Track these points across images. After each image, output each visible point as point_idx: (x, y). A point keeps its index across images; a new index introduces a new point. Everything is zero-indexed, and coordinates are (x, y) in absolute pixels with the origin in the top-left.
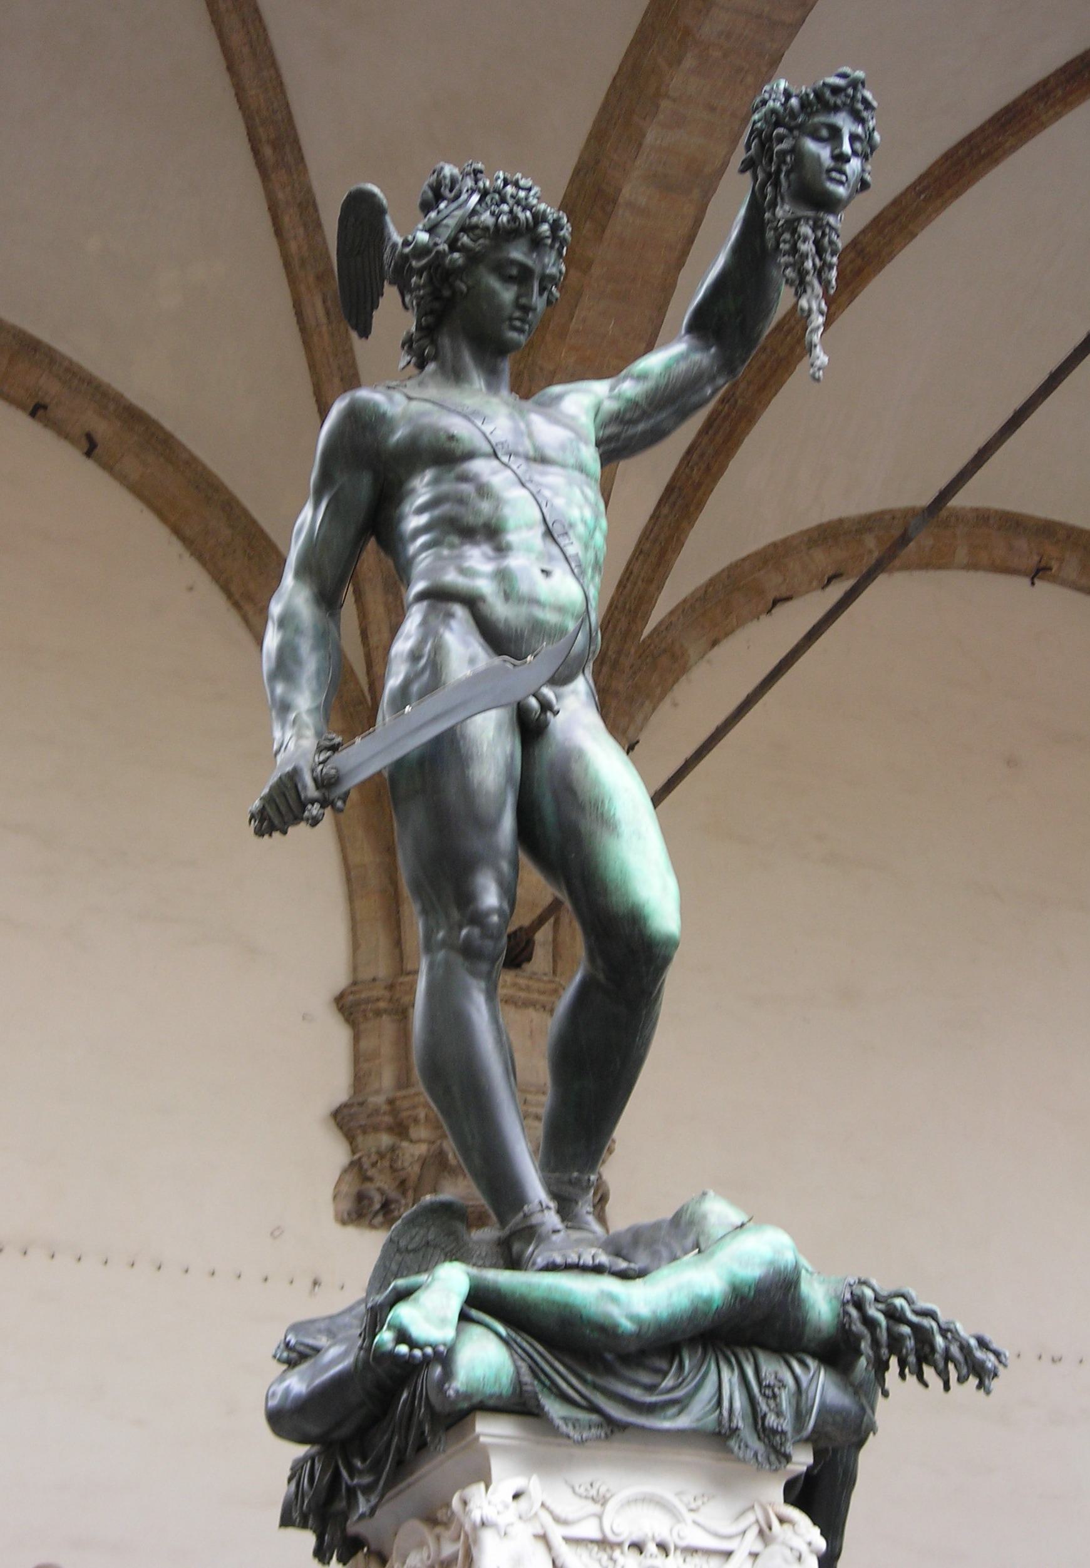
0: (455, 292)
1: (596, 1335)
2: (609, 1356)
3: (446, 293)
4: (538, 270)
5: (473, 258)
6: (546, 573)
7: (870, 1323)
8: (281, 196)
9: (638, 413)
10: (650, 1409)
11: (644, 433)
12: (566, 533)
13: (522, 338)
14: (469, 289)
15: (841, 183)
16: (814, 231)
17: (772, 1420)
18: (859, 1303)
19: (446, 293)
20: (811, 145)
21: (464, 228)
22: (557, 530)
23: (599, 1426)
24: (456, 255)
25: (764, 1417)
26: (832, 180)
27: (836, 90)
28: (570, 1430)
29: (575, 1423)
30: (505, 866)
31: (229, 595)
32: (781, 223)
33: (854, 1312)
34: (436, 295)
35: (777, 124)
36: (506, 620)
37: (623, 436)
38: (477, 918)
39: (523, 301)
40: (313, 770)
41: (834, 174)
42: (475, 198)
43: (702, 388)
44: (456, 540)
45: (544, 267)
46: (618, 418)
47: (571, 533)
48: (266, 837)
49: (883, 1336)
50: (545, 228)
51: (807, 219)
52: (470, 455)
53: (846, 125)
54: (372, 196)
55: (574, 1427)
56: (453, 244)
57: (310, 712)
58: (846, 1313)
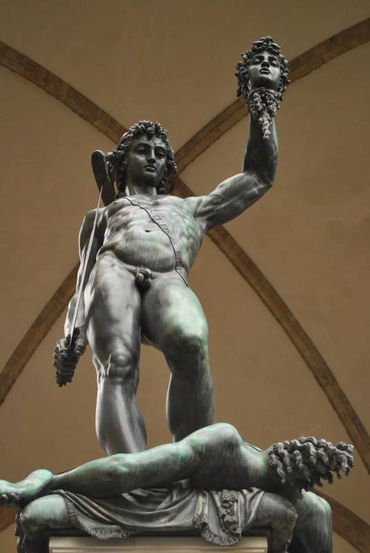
1: (108, 480)
2: (126, 495)
3: (122, 169)
4: (152, 145)
5: (127, 150)
6: (147, 231)
7: (281, 457)
8: (331, 394)
10: (151, 518)
11: (225, 207)
13: (154, 174)
14: (128, 162)
15: (267, 73)
17: (228, 518)
18: (276, 452)
20: (252, 67)
23: (118, 531)
25: (224, 516)
26: (263, 73)
27: (259, 45)
28: (93, 532)
29: (101, 530)
31: (353, 545)
33: (274, 456)
34: (119, 172)
36: (126, 247)
38: (114, 360)
39: (149, 158)
43: (251, 188)
45: (155, 144)
48: (63, 386)
49: (287, 460)
53: (266, 55)
54: (98, 152)
55: (101, 532)
58: (271, 458)
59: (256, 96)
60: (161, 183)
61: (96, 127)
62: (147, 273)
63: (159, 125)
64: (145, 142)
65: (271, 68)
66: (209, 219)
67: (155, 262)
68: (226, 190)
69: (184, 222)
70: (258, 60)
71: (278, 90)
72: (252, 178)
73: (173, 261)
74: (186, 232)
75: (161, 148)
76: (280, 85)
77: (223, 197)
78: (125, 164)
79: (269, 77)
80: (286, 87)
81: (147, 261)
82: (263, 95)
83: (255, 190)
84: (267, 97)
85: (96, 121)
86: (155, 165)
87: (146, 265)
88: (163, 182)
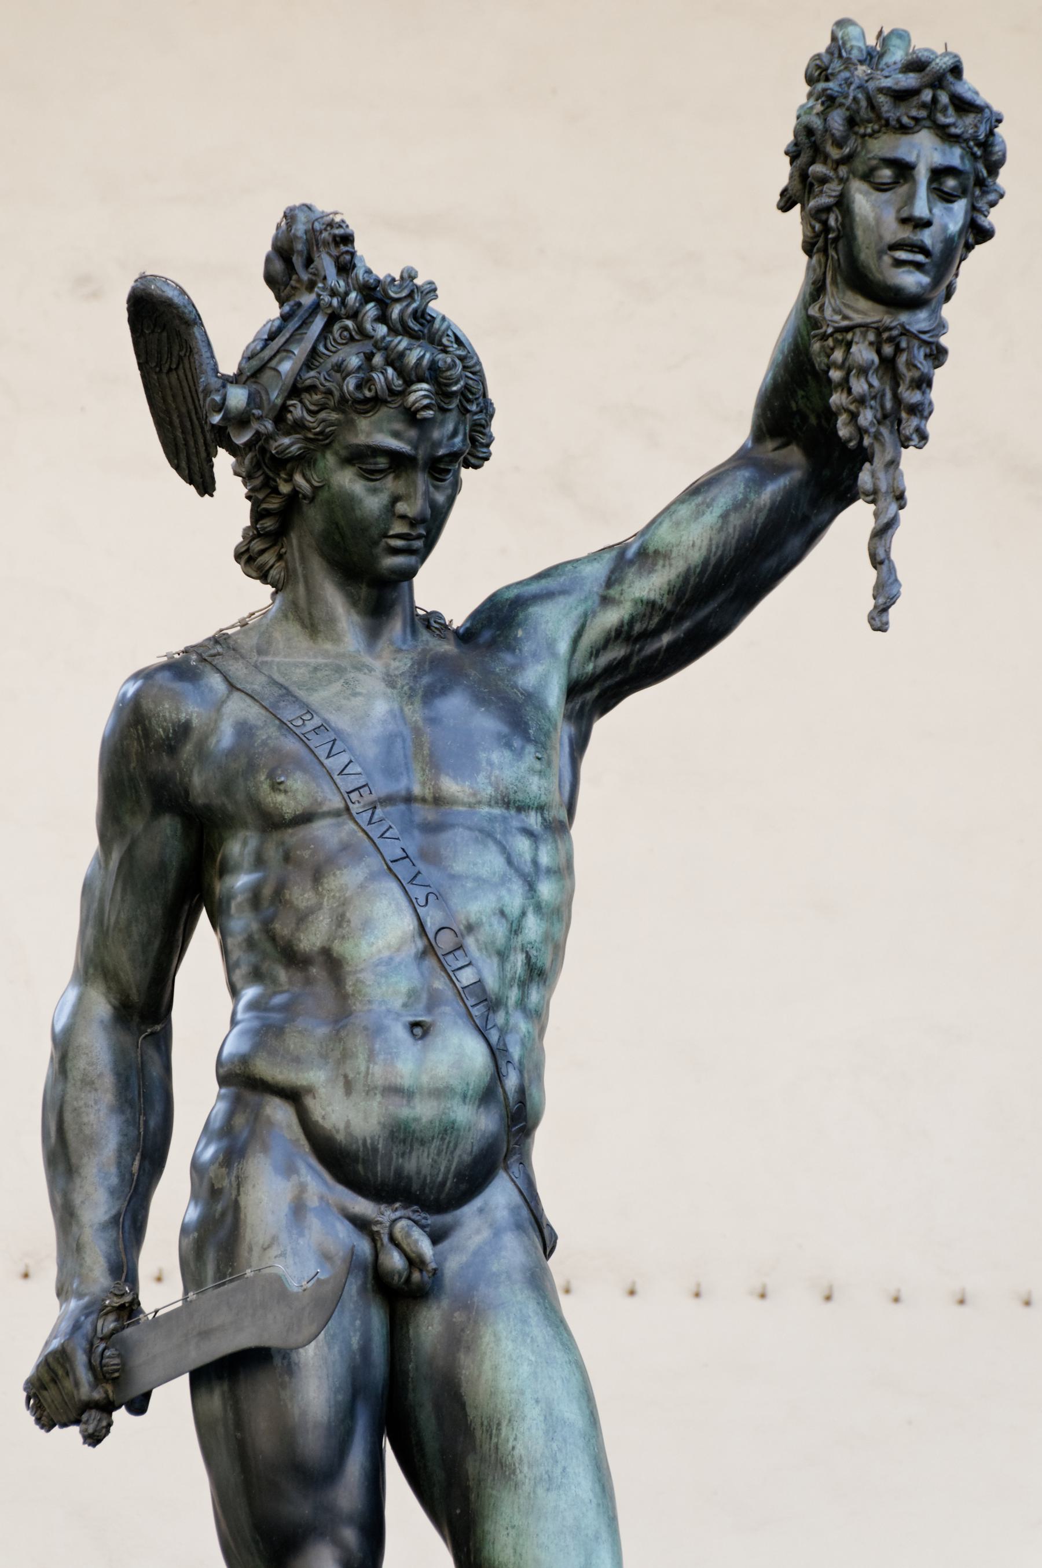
0: (295, 494)
4: (421, 454)
6: (419, 1029)
9: (656, 620)
11: (672, 646)
12: (460, 947)
14: (316, 489)
15: (919, 266)
16: (879, 352)
19: (285, 488)
21: (296, 391)
22: (445, 942)
24: (286, 441)
26: (899, 263)
27: (900, 96)
30: (350, 1535)
32: (830, 330)
35: (817, 153)
37: (635, 659)
40: (90, 1351)
41: (903, 255)
42: (318, 324)
44: (282, 975)
46: (620, 634)
47: (470, 942)
50: (421, 391)
51: (865, 327)
52: (306, 818)
53: (925, 150)
56: (280, 416)
57: (104, 1227)
59: (863, 371)
64: (394, 444)
67: (443, 1184)
68: (686, 577)
69: (538, 908)
77: (669, 606)
81: (415, 1187)
82: (888, 350)
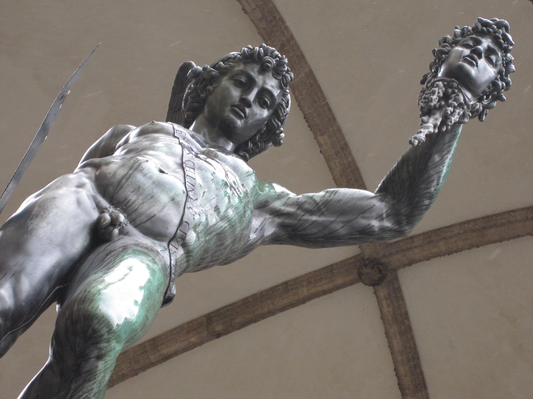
5: (223, 72)
11: (314, 222)
20: (459, 48)
26: (465, 60)
39: (244, 97)
45: (264, 82)
59: (438, 86)
60: (246, 143)
61: (320, 145)
62: (117, 218)
63: (286, 61)
65: (482, 62)
66: (282, 226)
67: (141, 214)
70: (471, 43)
71: (480, 100)
72: (380, 206)
73: (172, 230)
74: (223, 210)
75: (270, 93)
76: (484, 92)
78: (209, 90)
79: (473, 71)
80: (495, 104)
82: (450, 91)
83: (375, 224)
84: (453, 95)
85: (322, 135)
86: (247, 110)
87: (124, 211)
88: (250, 145)
